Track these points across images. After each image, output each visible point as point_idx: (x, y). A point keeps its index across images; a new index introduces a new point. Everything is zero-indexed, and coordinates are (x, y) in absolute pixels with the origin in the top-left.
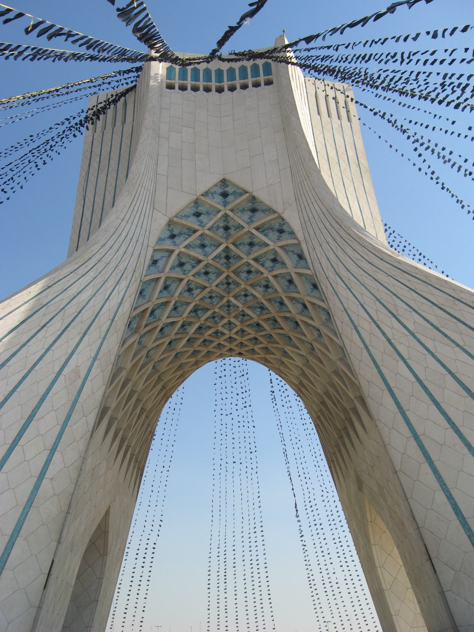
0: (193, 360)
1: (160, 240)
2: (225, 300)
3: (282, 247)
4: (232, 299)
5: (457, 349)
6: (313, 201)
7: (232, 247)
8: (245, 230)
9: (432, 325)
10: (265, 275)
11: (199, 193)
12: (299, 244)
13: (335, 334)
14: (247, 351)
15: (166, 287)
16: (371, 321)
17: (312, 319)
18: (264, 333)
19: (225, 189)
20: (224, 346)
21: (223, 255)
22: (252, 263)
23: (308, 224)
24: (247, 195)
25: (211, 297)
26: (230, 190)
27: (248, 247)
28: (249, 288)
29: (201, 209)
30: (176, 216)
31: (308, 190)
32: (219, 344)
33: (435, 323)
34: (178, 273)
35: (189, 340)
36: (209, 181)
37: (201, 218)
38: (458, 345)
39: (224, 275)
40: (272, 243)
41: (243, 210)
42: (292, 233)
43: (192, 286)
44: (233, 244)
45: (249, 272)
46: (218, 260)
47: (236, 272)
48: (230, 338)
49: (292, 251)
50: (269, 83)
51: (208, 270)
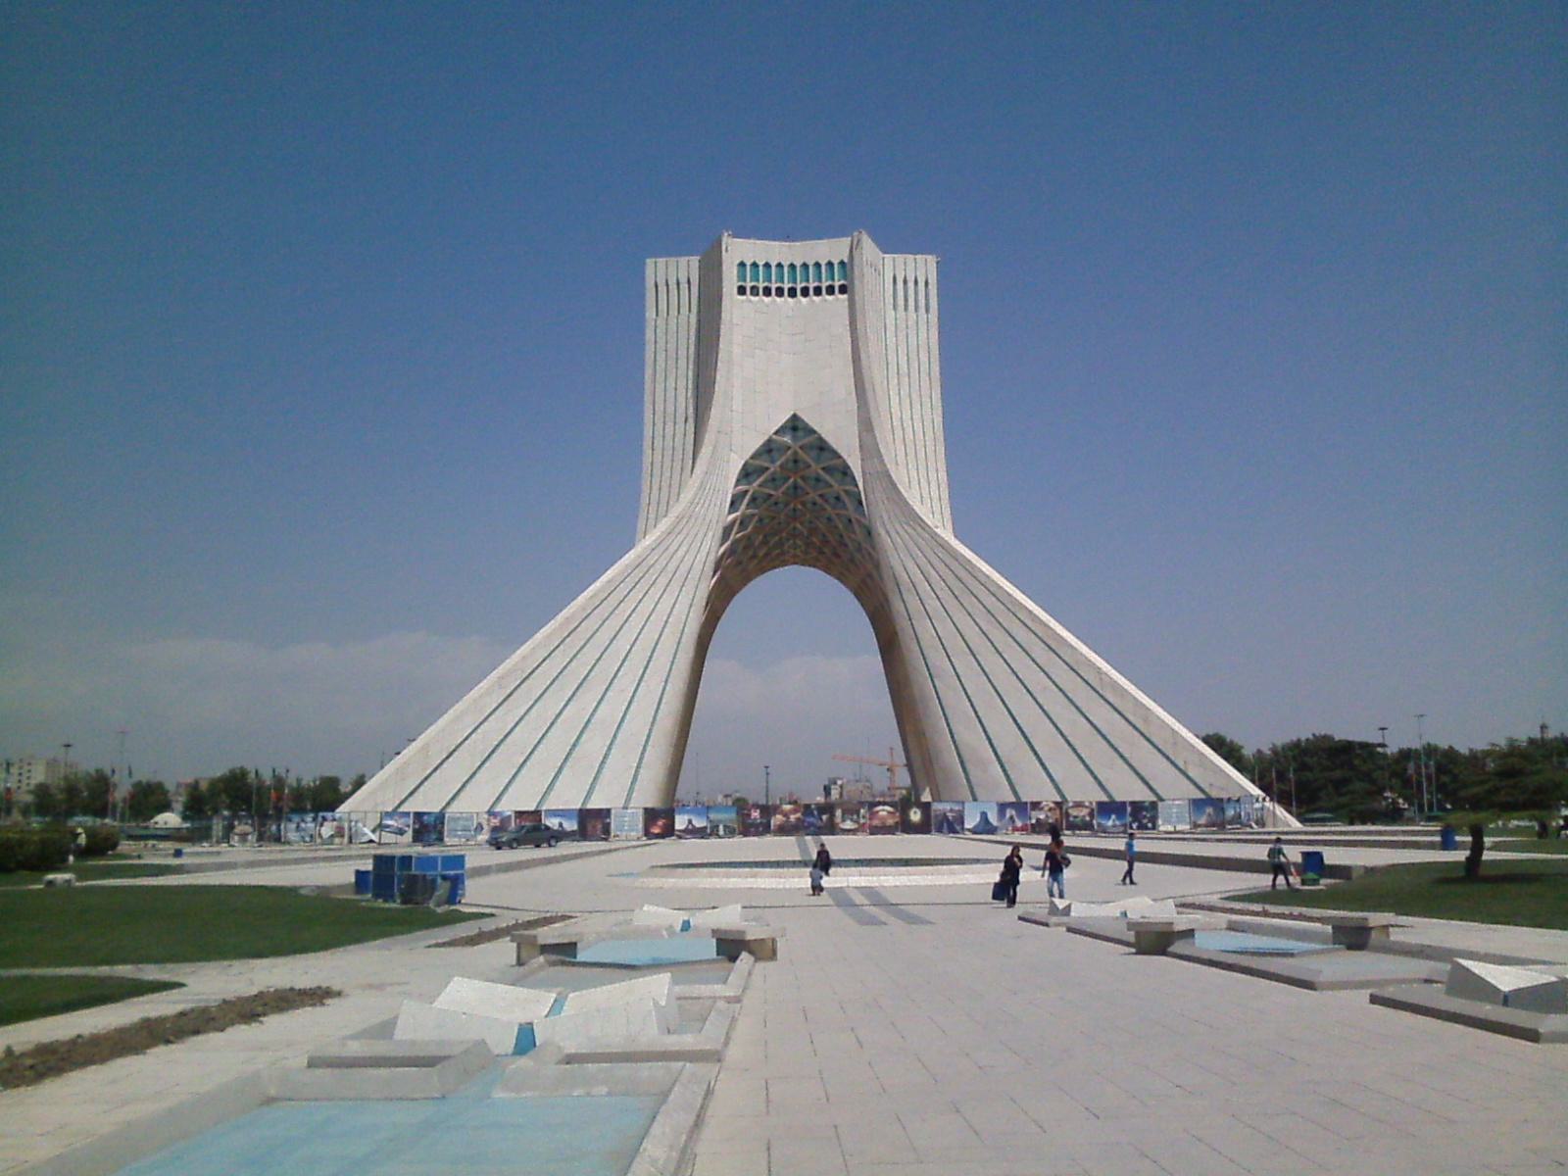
1: (738, 482)
2: (792, 526)
4: (798, 526)
11: (773, 431)
15: (741, 523)
19: (795, 425)
26: (800, 425)
29: (773, 446)
30: (752, 458)
36: (783, 418)
38: (970, 614)
40: (836, 485)
42: (854, 478)
44: (803, 478)
45: (815, 504)
47: (803, 504)
50: (843, 289)
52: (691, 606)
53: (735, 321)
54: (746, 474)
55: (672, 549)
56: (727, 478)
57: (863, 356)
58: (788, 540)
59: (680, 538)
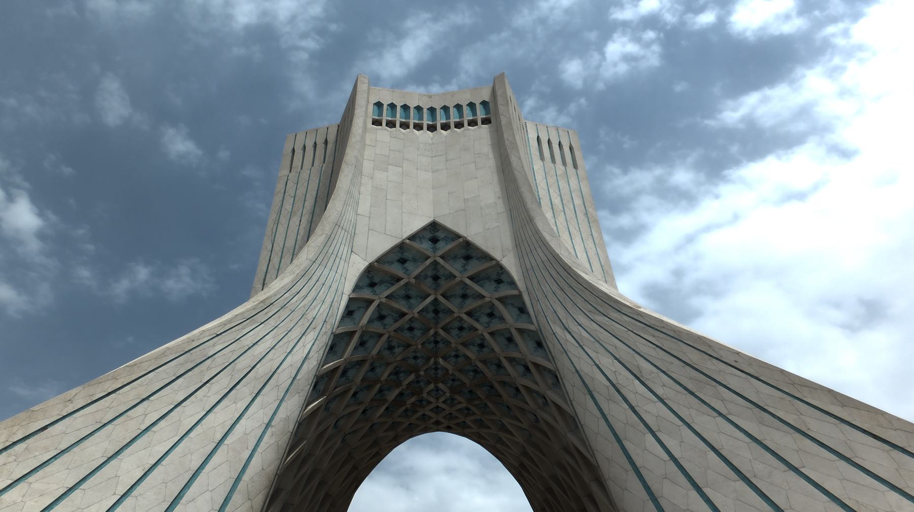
0: (391, 434)
1: (357, 288)
3: (499, 299)
5: (720, 419)
6: (536, 246)
7: (441, 299)
8: (458, 279)
9: (686, 388)
10: (480, 332)
12: (520, 296)
13: (565, 399)
14: (457, 424)
15: (362, 343)
16: (608, 384)
17: (536, 383)
18: (477, 402)
20: (430, 418)
21: (432, 308)
22: (465, 317)
23: (531, 272)
24: (461, 240)
25: (415, 358)
26: (440, 235)
27: (460, 300)
28: (460, 347)
29: (407, 255)
31: (530, 233)
32: (424, 415)
33: (690, 387)
34: (377, 327)
35: (387, 408)
36: (418, 224)
37: (406, 265)
38: (720, 414)
39: (432, 332)
41: (455, 258)
42: (512, 283)
43: (393, 344)
44: (443, 295)
46: (425, 314)
48: (437, 407)
49: (512, 304)
50: (486, 121)
51: (413, 325)
52: (268, 425)
53: (368, 142)
54: (372, 277)
55: (248, 341)
56: (344, 277)
57: (513, 159)
58: (429, 383)
59: (261, 331)
